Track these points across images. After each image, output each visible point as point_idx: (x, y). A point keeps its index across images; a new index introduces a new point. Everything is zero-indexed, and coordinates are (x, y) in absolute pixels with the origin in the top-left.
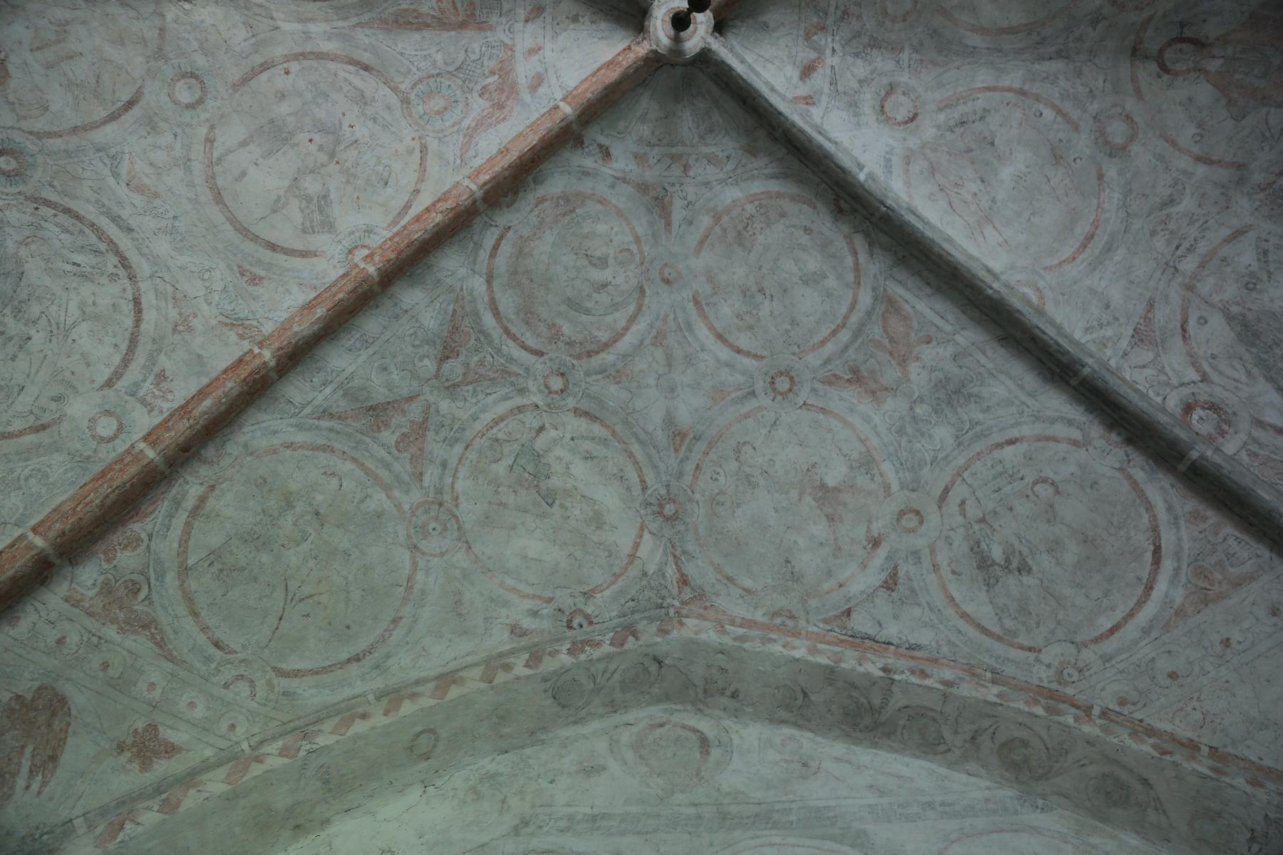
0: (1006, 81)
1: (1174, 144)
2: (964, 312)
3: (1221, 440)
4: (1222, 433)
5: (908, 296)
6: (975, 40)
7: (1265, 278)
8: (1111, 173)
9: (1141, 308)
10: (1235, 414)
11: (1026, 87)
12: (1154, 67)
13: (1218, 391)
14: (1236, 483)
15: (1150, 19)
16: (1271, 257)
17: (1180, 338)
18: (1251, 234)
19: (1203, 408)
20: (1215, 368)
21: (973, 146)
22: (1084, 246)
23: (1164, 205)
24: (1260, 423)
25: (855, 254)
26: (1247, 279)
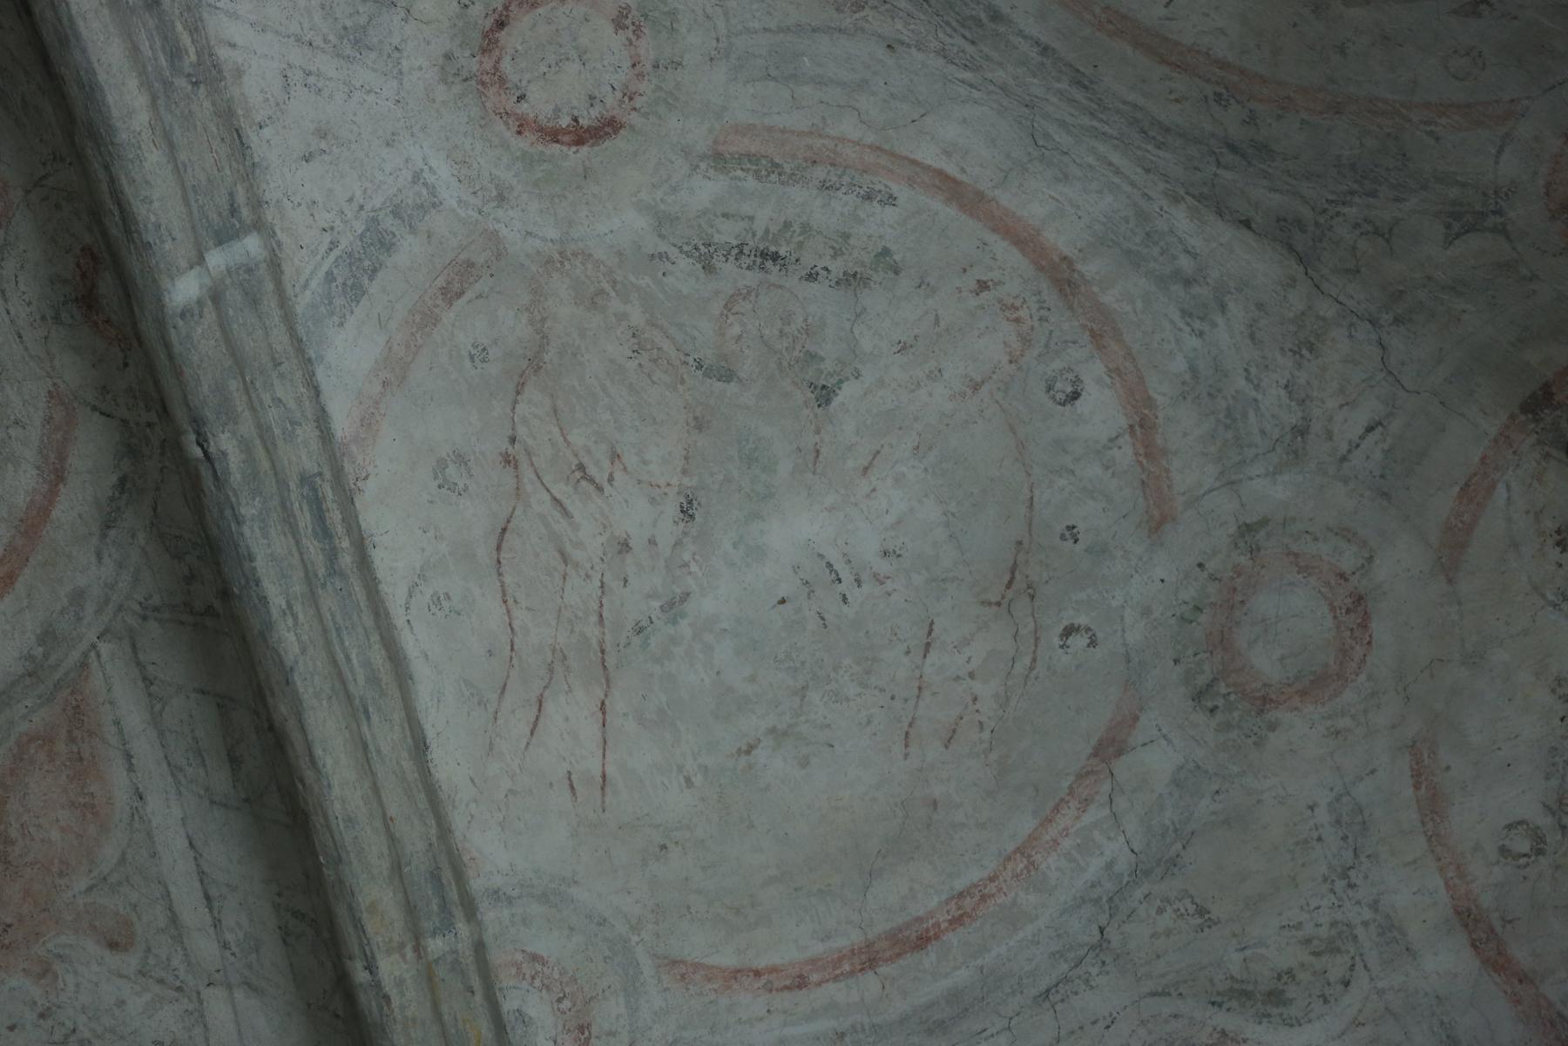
0: (1033, 202)
1: (1433, 805)
2: (285, 934)
5: (145, 748)
8: (1155, 760)
11: (1090, 268)
22: (868, 958)
23: (1240, 994)
25: (56, 476)
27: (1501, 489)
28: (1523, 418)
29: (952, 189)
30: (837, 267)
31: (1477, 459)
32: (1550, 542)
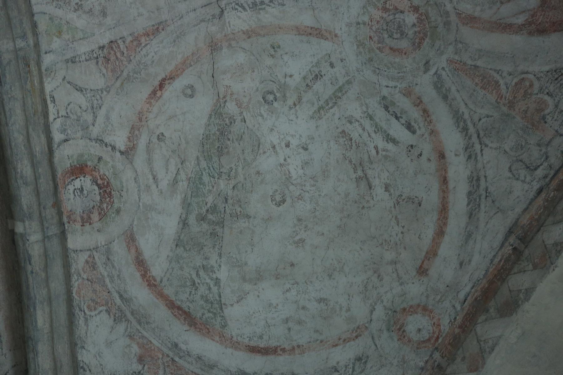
3: (78, 226)
4: (86, 220)
7: (290, 102)
9: (142, 24)
10: (118, 211)
13: (128, 175)
14: (28, 288)
16: (318, 86)
17: (149, 90)
18: (327, 46)
19: (95, 181)
20: (149, 150)
24: (130, 239)
26: (274, 87)
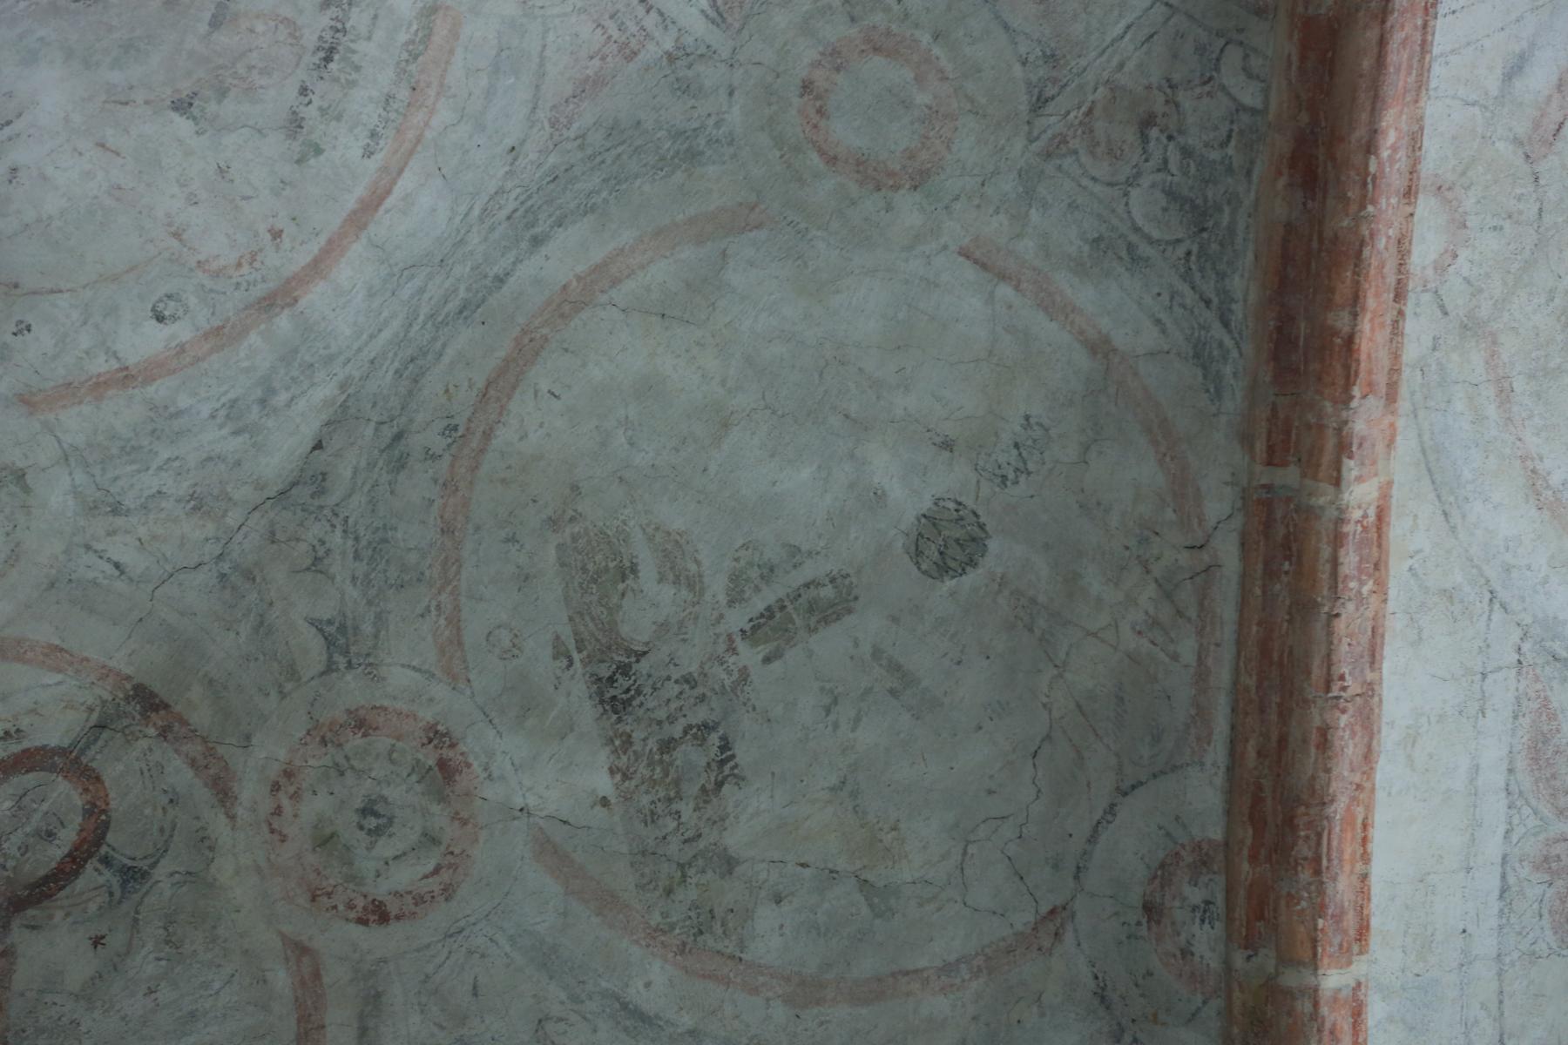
0: (354, 270)
6: (563, 258)
11: (284, 322)
12: (54, 732)
15: (223, 793)
21: (224, 39)
27: (59, 677)
28: (128, 686)
29: (372, 203)
30: (311, 113)
31: (85, 654)
32: (8, 726)
